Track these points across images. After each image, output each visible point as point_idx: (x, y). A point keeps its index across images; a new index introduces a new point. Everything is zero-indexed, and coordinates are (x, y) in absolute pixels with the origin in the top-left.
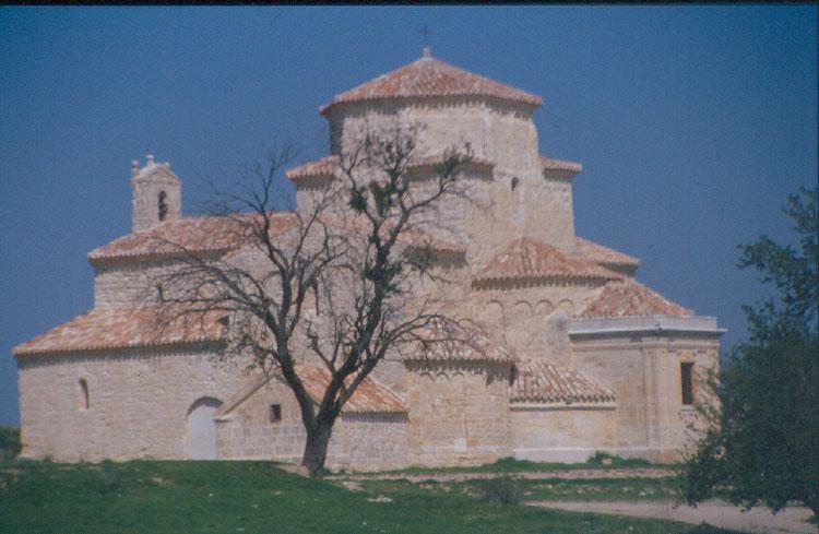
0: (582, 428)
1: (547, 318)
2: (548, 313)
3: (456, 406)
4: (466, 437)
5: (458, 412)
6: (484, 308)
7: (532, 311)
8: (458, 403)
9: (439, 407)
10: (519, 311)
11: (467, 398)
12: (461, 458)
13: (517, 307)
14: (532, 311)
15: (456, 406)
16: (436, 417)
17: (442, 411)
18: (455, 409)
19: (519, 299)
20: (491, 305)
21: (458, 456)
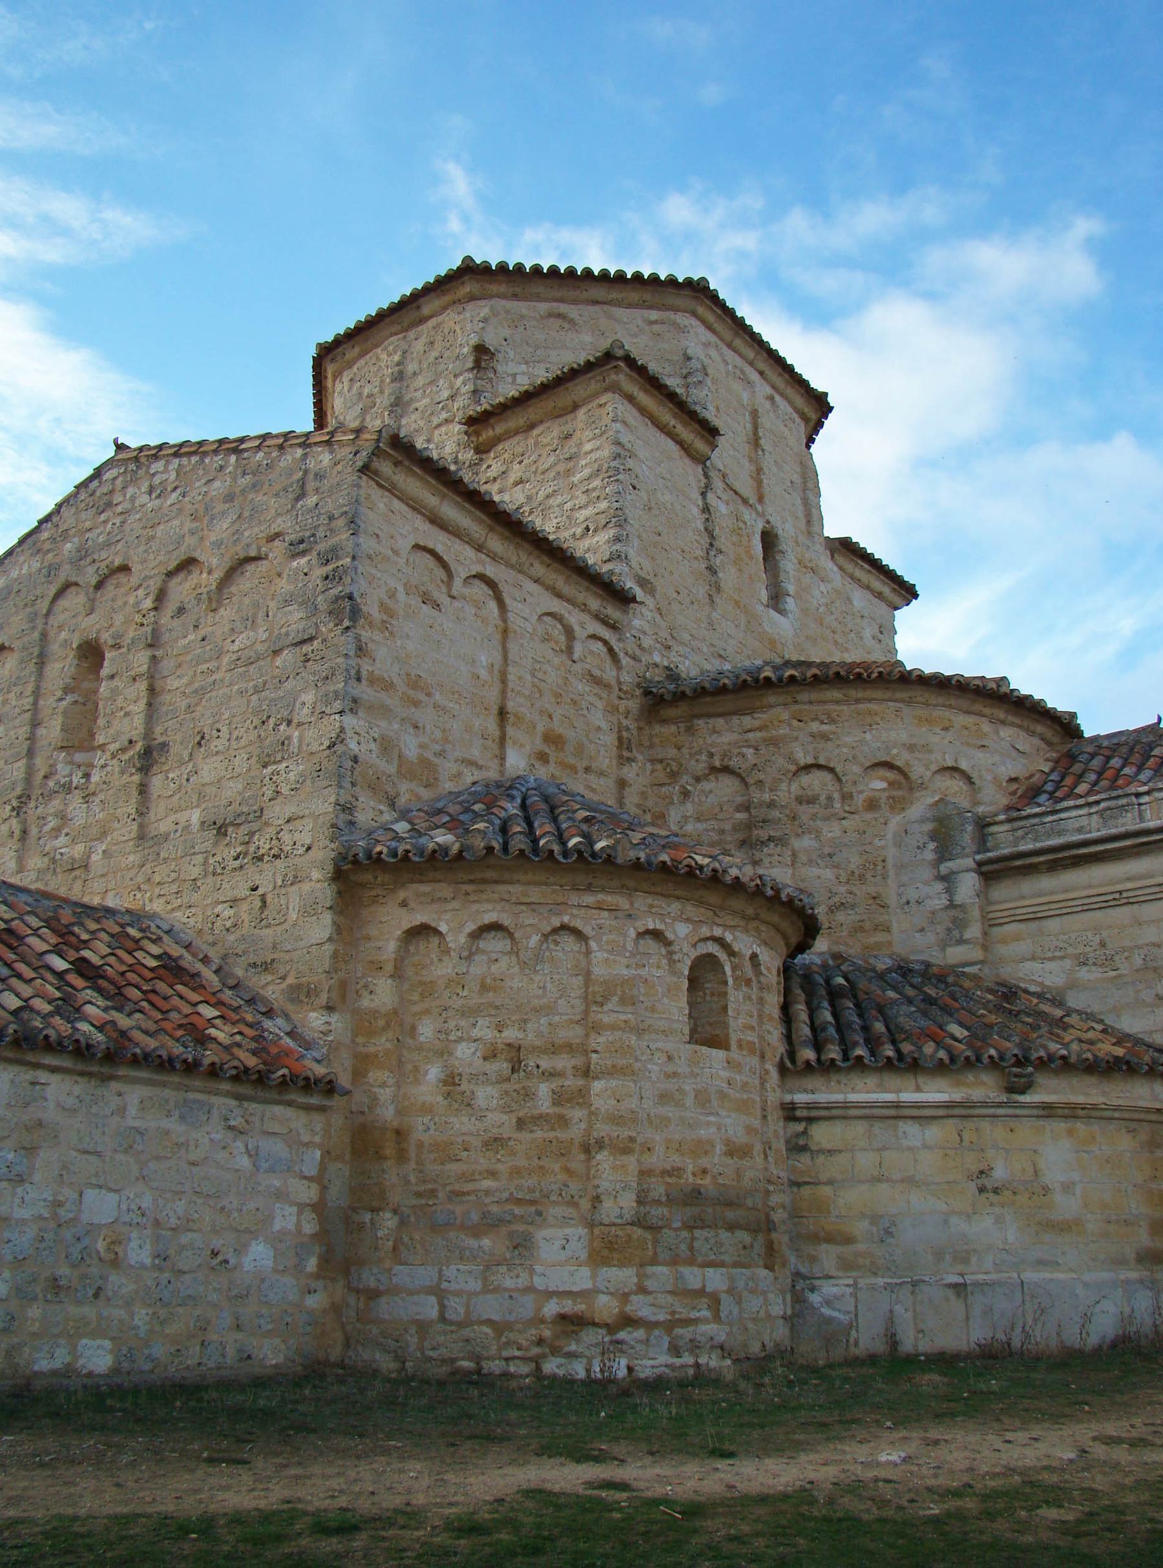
0: (1068, 1187)
1: (895, 821)
2: (898, 805)
3: (552, 1074)
4: (591, 1225)
5: (559, 1098)
6: (686, 794)
7: (846, 797)
8: (563, 1062)
9: (473, 1077)
10: (800, 800)
11: (599, 1041)
12: (563, 1318)
13: (794, 787)
14: (846, 797)
15: (552, 1074)
16: (462, 1124)
17: (486, 1095)
18: (544, 1090)
19: (804, 759)
20: (706, 786)
21: (551, 1308)
